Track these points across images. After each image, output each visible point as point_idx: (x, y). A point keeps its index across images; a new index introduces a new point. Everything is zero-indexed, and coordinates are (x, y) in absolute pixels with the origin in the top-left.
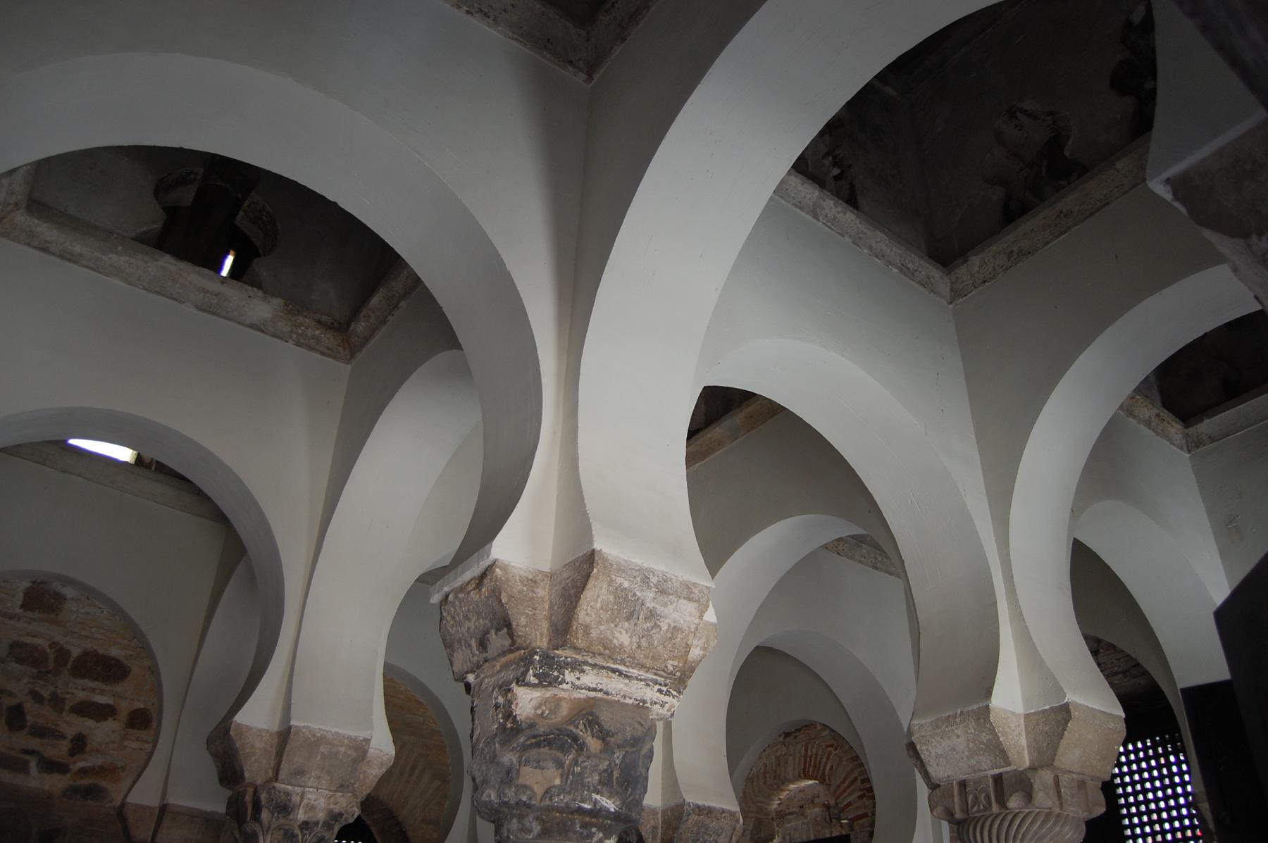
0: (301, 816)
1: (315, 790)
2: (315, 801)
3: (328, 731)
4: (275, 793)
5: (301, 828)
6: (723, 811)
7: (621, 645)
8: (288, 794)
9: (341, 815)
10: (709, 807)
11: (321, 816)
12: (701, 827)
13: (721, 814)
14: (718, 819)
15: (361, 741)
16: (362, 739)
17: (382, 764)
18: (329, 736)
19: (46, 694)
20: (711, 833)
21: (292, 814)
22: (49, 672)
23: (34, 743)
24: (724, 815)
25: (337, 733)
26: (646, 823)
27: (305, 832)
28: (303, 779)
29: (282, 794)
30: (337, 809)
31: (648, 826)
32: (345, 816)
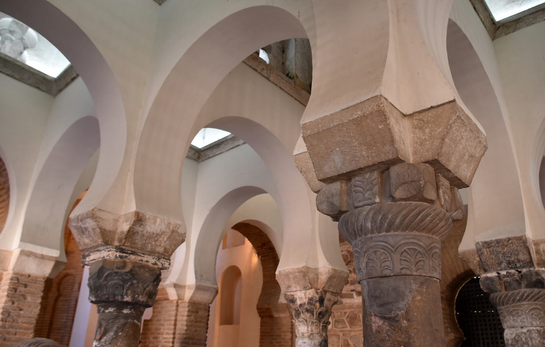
0: (299, 302)
1: (300, 291)
2: (301, 295)
3: (289, 269)
4: (287, 296)
5: (300, 307)
6: (509, 239)
7: (87, 243)
8: (292, 295)
9: (312, 298)
10: (496, 240)
11: (306, 301)
12: (497, 254)
13: (508, 241)
14: (507, 246)
15: (301, 268)
16: (301, 267)
17: (326, 273)
18: (290, 270)
19: (351, 269)
20: (509, 255)
21: (296, 302)
22: (350, 261)
23: (352, 287)
24: (510, 242)
25: (293, 268)
26: (473, 260)
27: (301, 308)
28: (291, 289)
29: (290, 296)
30: (310, 296)
31: (475, 262)
32: (314, 298)
